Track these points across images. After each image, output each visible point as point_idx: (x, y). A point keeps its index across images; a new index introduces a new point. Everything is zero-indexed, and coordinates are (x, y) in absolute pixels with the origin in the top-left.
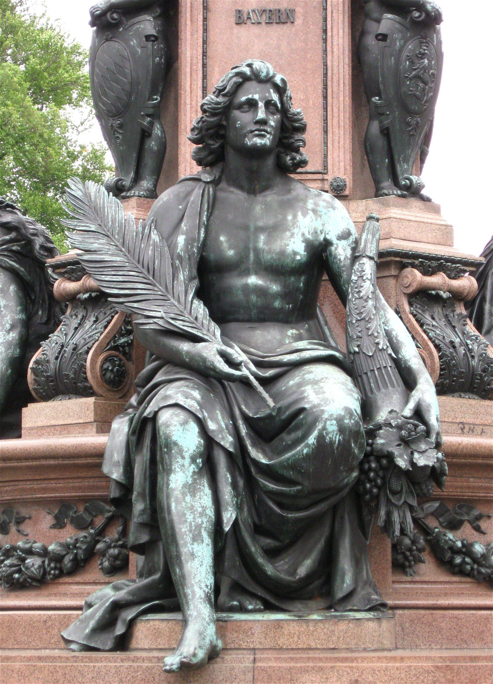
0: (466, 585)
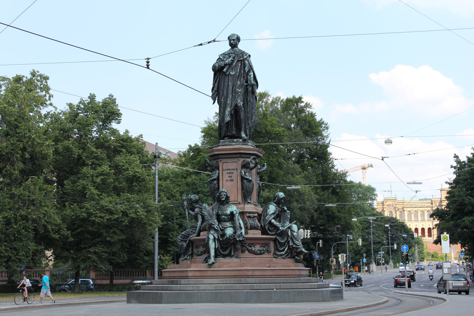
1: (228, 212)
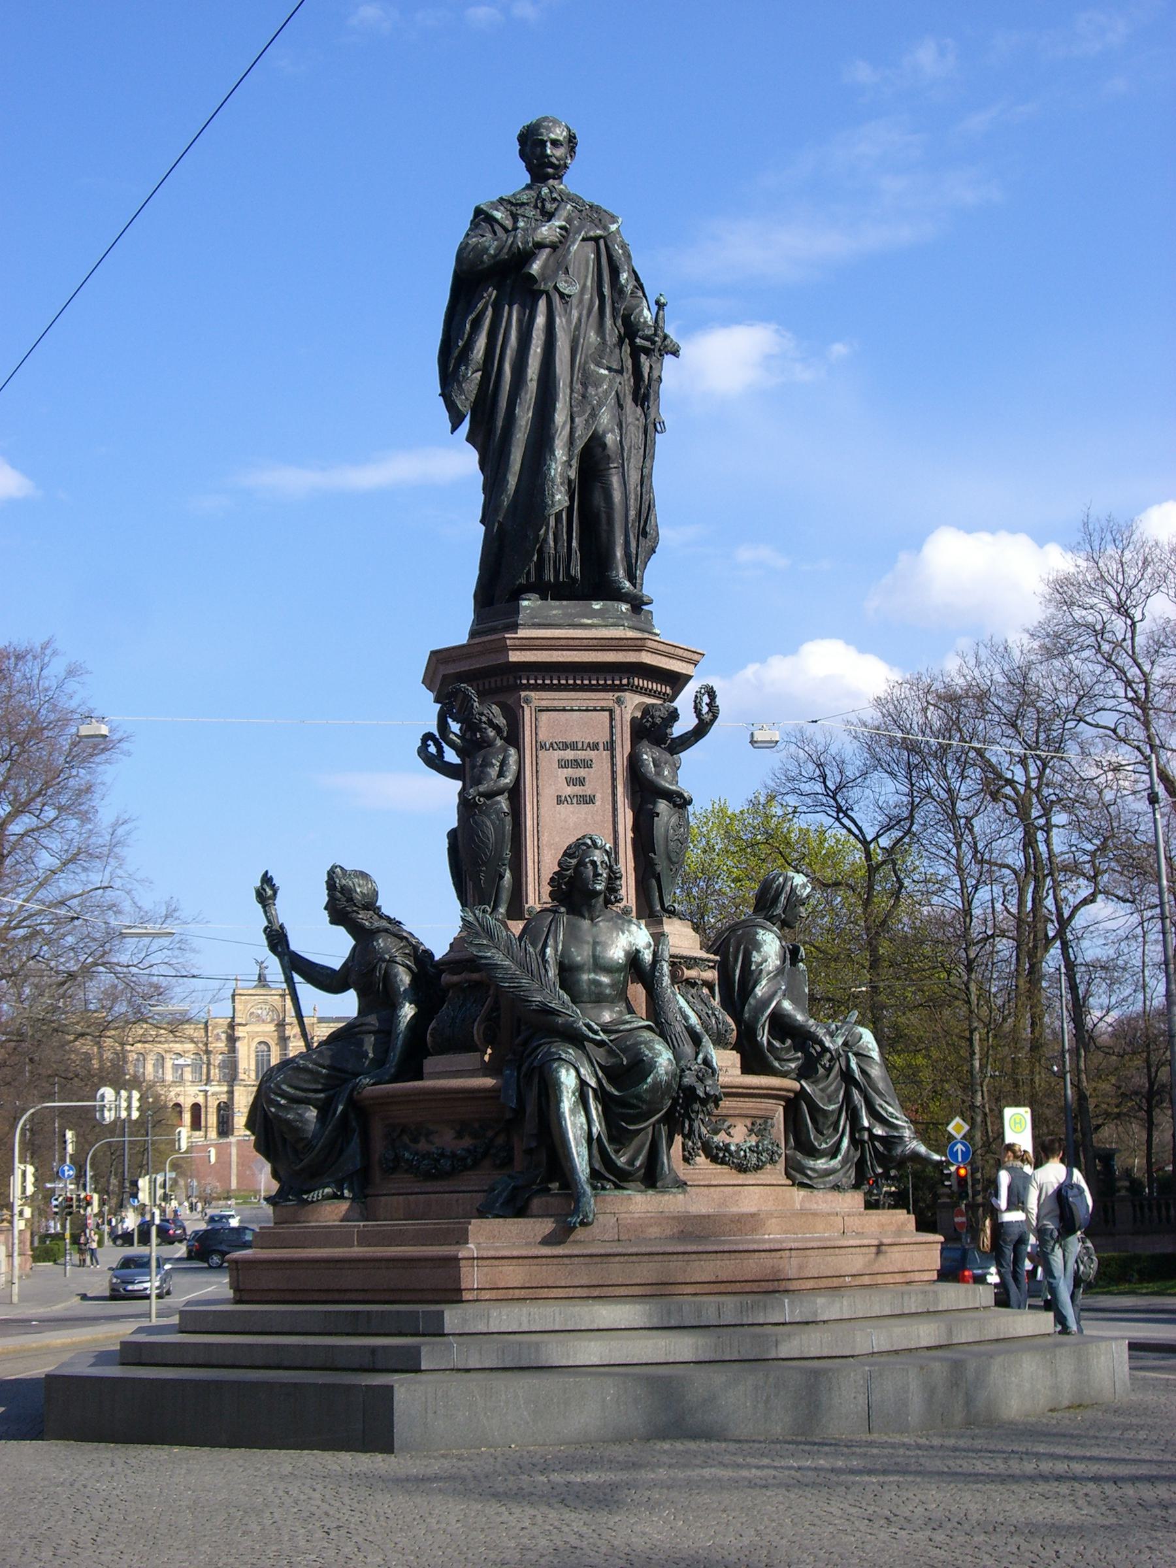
0: (725, 1169)
1: (617, 952)
